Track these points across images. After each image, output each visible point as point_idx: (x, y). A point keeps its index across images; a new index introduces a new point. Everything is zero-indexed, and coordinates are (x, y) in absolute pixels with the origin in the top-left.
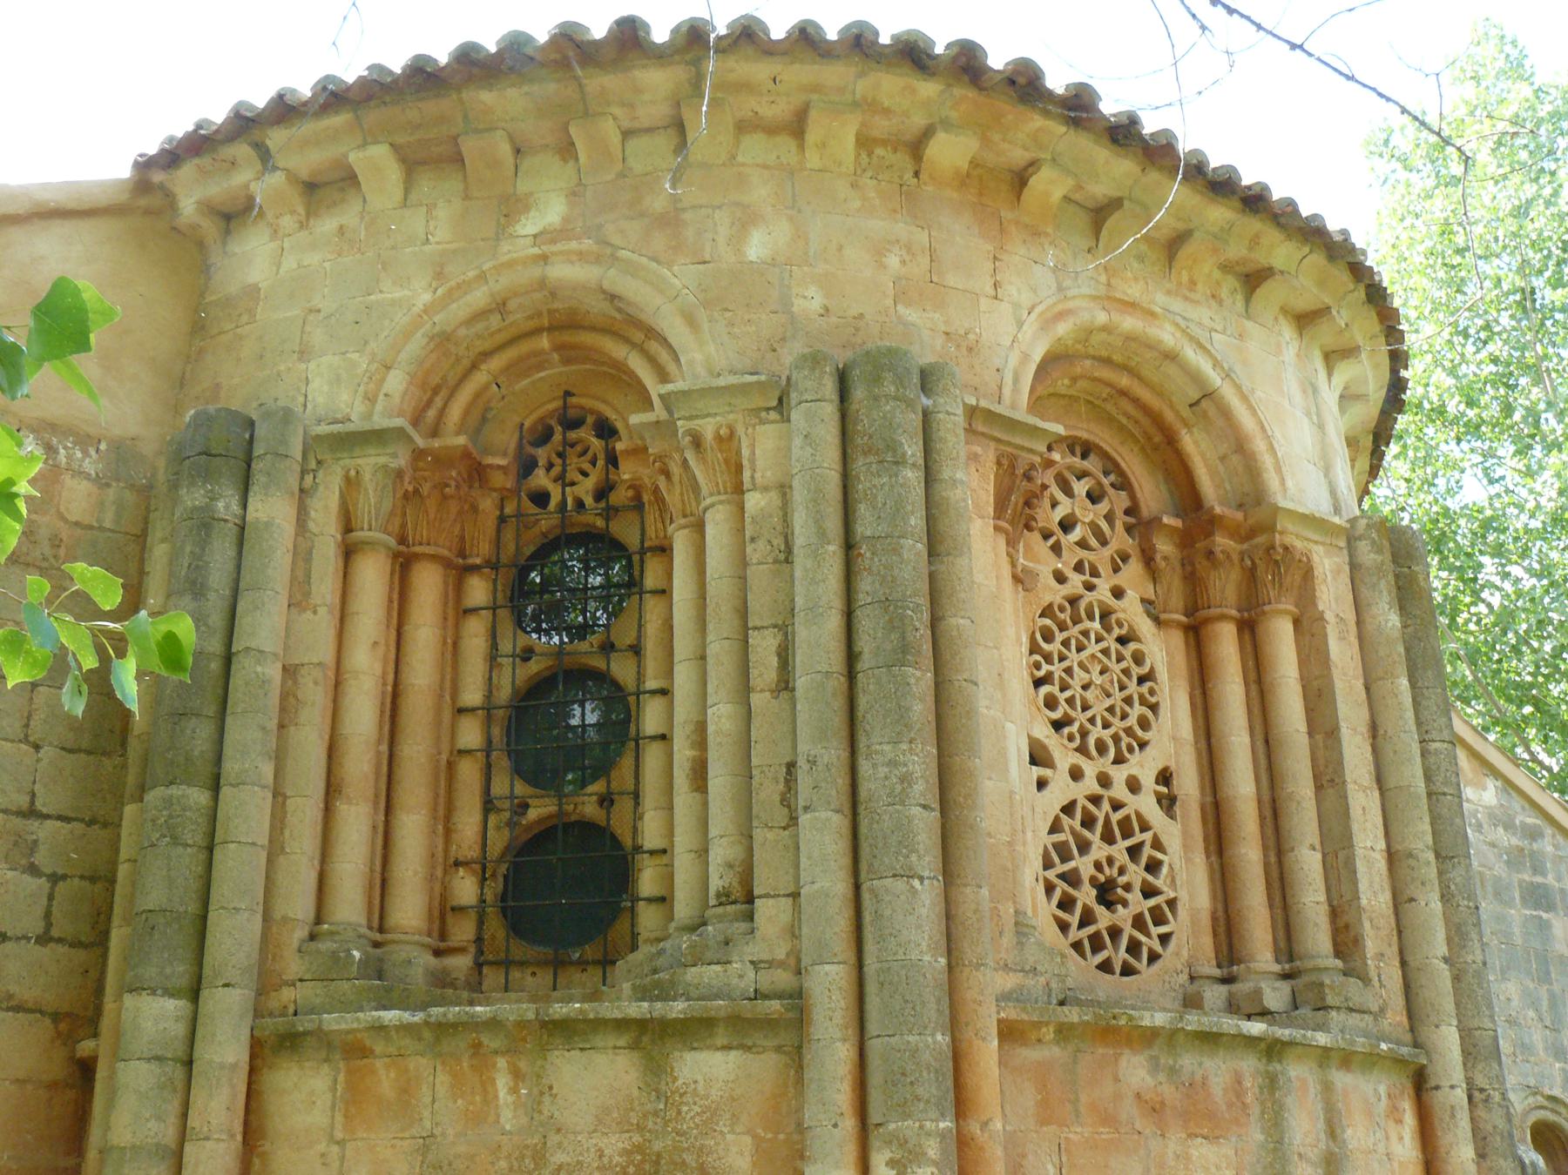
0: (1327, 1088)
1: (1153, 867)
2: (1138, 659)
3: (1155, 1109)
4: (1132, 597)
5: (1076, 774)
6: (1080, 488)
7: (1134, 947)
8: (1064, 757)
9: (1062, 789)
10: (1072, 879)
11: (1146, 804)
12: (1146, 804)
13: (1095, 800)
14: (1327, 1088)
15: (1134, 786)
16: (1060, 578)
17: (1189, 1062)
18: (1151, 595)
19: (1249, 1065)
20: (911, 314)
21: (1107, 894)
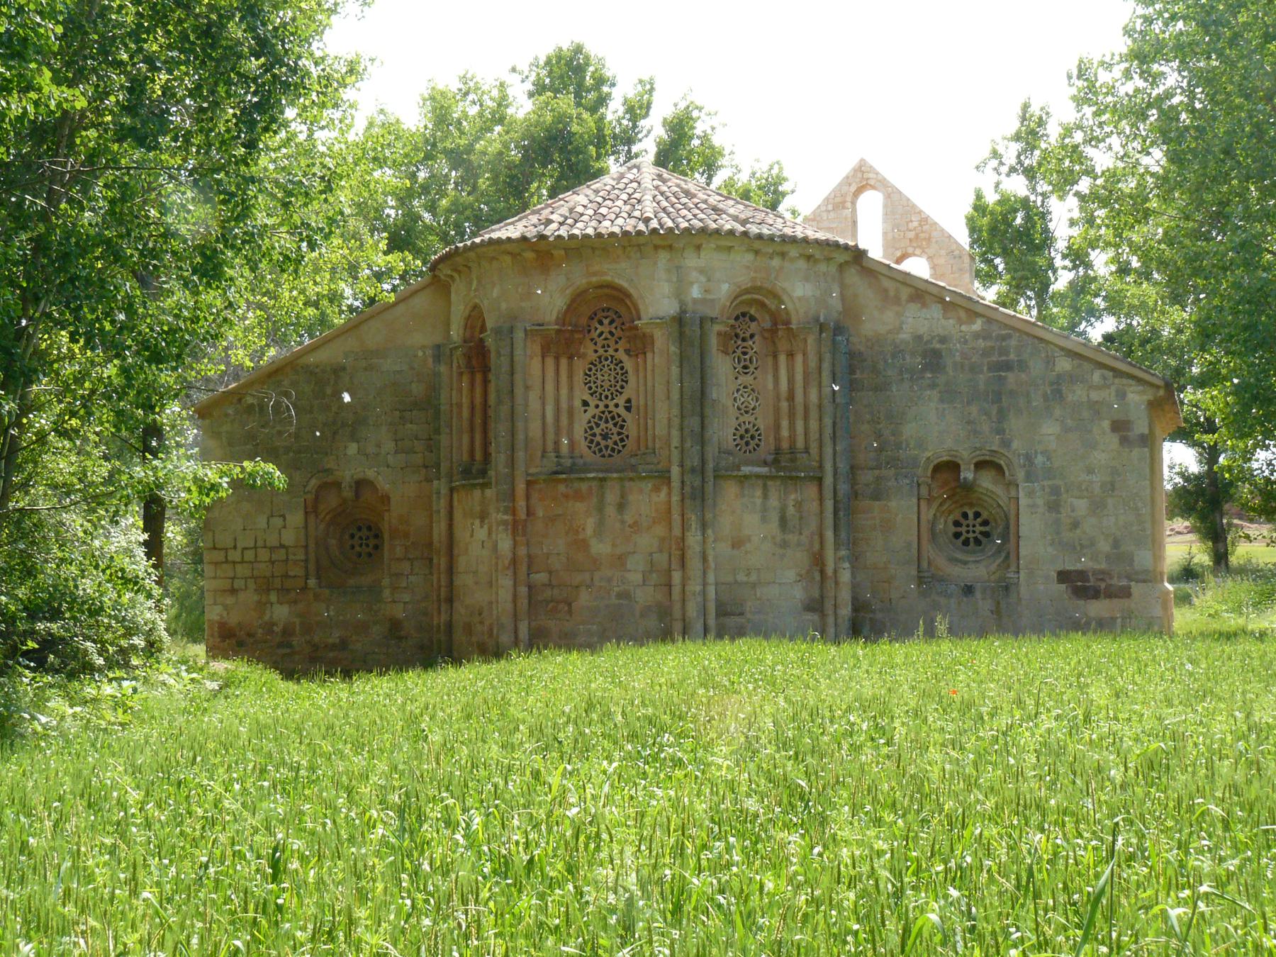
0: (623, 488)
1: (622, 427)
2: (622, 368)
3: (566, 496)
4: (621, 351)
5: (597, 406)
6: (606, 322)
7: (613, 450)
8: (592, 402)
9: (592, 411)
10: (594, 435)
11: (621, 410)
12: (621, 410)
13: (603, 412)
14: (623, 488)
15: (617, 406)
16: (596, 351)
17: (576, 485)
18: (628, 346)
19: (594, 484)
20: (523, 304)
21: (605, 437)
